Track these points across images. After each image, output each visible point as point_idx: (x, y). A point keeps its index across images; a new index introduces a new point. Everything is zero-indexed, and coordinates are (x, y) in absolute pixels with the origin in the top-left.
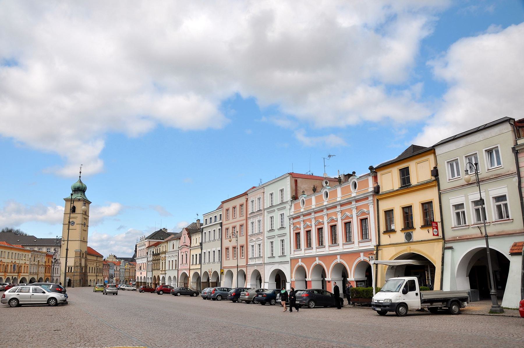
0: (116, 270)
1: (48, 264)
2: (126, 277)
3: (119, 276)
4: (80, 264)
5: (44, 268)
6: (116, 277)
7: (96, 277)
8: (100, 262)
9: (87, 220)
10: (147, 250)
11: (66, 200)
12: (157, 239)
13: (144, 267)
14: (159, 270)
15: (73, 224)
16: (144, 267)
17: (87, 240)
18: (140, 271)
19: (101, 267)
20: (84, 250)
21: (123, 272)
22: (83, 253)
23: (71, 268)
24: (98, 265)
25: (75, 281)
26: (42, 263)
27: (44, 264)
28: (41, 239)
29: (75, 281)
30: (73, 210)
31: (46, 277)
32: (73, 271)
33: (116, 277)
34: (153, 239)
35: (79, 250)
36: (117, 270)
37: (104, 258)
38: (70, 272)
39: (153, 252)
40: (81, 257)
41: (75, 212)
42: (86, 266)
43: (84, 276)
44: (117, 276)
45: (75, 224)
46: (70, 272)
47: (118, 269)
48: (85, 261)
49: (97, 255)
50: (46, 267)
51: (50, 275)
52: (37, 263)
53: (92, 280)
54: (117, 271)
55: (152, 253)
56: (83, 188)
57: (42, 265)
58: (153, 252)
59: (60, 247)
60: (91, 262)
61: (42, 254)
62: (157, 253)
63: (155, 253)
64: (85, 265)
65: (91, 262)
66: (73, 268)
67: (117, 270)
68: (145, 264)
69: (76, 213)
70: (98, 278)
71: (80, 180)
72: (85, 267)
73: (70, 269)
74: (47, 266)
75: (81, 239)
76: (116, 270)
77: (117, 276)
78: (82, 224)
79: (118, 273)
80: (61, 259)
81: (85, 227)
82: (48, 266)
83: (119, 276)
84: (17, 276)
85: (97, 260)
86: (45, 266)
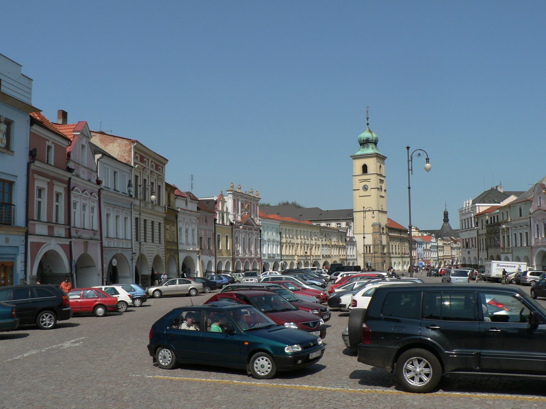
0: (425, 248)
4: (381, 241)
10: (476, 219)
12: (489, 203)
13: (474, 243)
14: (498, 247)
16: (474, 243)
18: (468, 250)
20: (384, 222)
22: (383, 227)
23: (370, 247)
28: (328, 211)
30: (365, 169)
32: (371, 252)
34: (484, 202)
35: (378, 224)
38: (368, 252)
39: (487, 222)
41: (367, 173)
42: (388, 245)
46: (368, 252)
53: (396, 263)
55: (484, 223)
58: (487, 222)
59: (353, 221)
62: (493, 222)
63: (489, 222)
66: (371, 247)
68: (474, 240)
69: (368, 173)
76: (425, 248)
78: (378, 189)
80: (355, 236)
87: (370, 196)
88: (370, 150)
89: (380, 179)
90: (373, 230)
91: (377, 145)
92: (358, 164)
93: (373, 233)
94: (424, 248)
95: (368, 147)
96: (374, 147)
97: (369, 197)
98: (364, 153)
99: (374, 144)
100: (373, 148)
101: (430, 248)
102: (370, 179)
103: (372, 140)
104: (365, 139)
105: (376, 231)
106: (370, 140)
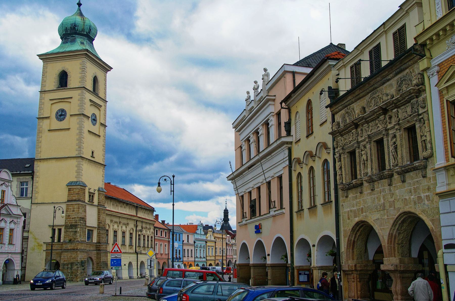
0: (186, 242)
2: (208, 258)
3: (193, 256)
6: (188, 257)
9: (102, 109)
15: (62, 117)
21: (203, 246)
33: (188, 257)
36: (188, 242)
37: (155, 213)
43: (97, 254)
44: (190, 255)
45: (68, 115)
47: (191, 242)
48: (99, 212)
54: (188, 244)
56: (86, 27)
67: (188, 242)
69: (68, 87)
70: (142, 258)
71: (80, 10)
72: (99, 228)
76: (186, 242)
77: (190, 255)
79: (190, 248)
81: (94, 125)
83: (193, 256)
87: (69, 129)
90: (69, 195)
91: (93, 42)
93: (68, 201)
94: (183, 241)
95: (73, 41)
96: (85, 43)
97: (67, 132)
98: (64, 50)
99: (86, 38)
101: (195, 242)
103: (83, 30)
104: (69, 26)
106: (80, 28)
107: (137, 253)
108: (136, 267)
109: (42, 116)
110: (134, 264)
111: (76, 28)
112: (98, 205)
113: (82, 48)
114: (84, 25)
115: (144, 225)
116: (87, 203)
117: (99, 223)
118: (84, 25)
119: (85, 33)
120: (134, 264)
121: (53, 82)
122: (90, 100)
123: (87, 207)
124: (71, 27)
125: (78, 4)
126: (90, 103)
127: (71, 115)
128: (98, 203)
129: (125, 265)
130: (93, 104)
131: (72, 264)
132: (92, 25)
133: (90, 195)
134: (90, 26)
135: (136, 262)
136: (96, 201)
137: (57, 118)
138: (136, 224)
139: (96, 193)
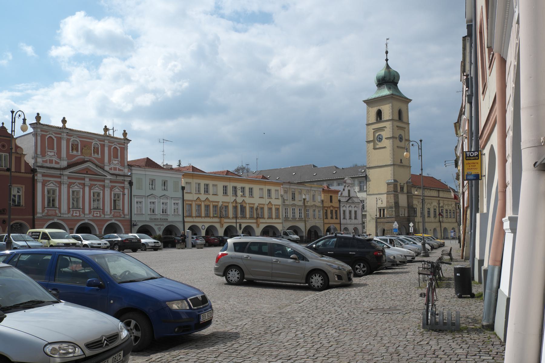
1: (330, 204)
5: (322, 211)
7: (439, 224)
8: (444, 199)
11: (369, 102)
17: (410, 164)
19: (450, 208)
23: (384, 210)
24: (441, 205)
25: (389, 230)
26: (313, 203)
27: (320, 204)
29: (389, 230)
30: (379, 114)
31: (327, 227)
40: (397, 192)
41: (381, 118)
46: (382, 216)
49: (438, 189)
50: (326, 209)
51: (338, 221)
52: (301, 203)
57: (316, 206)
59: (366, 179)
60: (431, 199)
61: (312, 189)
64: (408, 206)
65: (431, 199)
69: (383, 120)
73: (382, 213)
74: (328, 207)
75: (393, 162)
82: (330, 207)
84: (235, 224)
85: (439, 197)
86: (324, 207)
88: (385, 92)
89: (397, 126)
92: (374, 110)
100: (389, 89)
102: (385, 127)
103: (390, 79)
104: (381, 78)
105: (391, 190)
106: (387, 79)
107: (440, 222)
108: (440, 231)
109: (369, 140)
110: (438, 230)
111: (385, 79)
112: (407, 193)
113: (389, 93)
114: (390, 76)
115: (446, 202)
116: (399, 193)
117: (408, 204)
118: (390, 76)
119: (391, 81)
120: (438, 230)
121: (373, 119)
122: (397, 126)
123: (399, 195)
124: (382, 79)
125: (386, 60)
126: (397, 128)
127: (385, 138)
128: (407, 191)
129: (430, 230)
130: (399, 128)
131: (391, 230)
132: (396, 74)
133: (401, 188)
134: (394, 76)
135: (440, 228)
136: (405, 190)
137: (377, 140)
138: (439, 202)
139: (406, 185)
